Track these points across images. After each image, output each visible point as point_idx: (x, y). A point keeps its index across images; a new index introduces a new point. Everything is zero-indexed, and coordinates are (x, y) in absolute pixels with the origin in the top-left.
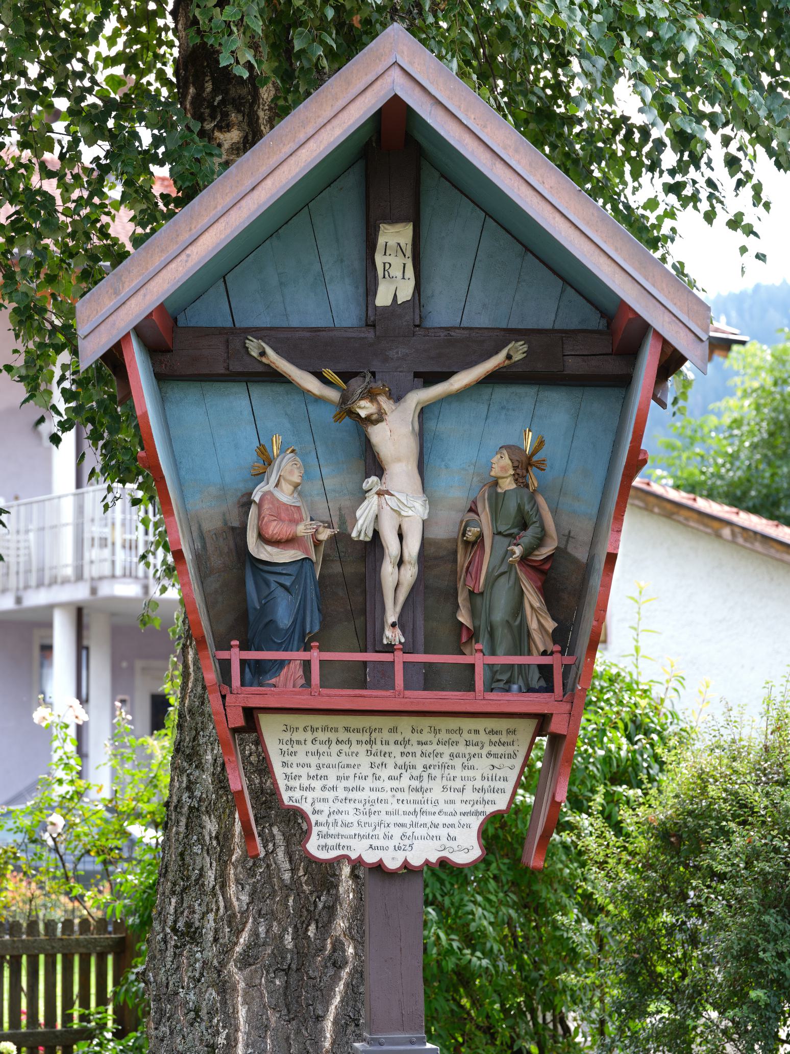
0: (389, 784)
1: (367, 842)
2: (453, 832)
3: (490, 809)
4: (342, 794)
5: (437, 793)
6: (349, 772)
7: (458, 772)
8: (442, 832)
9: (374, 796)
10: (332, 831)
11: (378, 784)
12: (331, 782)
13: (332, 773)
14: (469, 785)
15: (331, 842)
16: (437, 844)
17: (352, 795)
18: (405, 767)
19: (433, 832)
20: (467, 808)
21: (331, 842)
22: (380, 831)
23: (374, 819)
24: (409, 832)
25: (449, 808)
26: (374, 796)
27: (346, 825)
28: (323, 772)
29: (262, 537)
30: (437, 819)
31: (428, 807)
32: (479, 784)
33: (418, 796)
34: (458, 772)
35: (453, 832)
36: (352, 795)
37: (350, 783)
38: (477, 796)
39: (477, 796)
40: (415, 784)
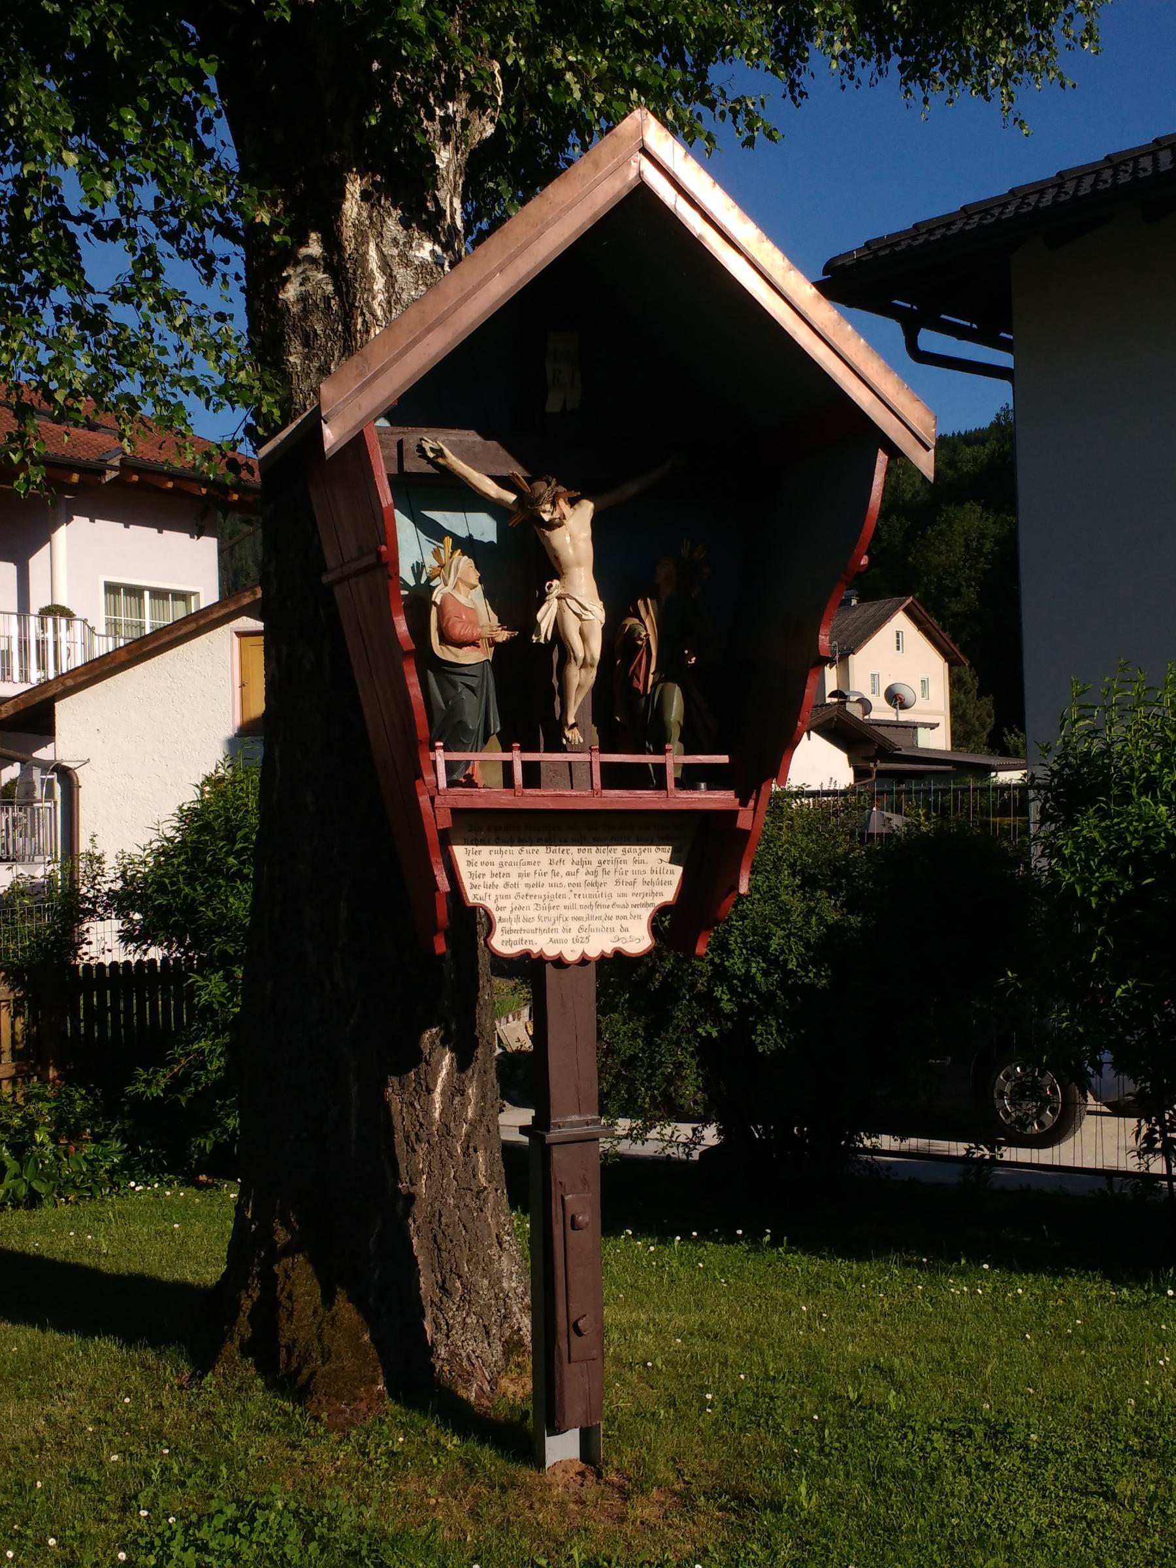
0: (567, 880)
1: (547, 936)
2: (625, 923)
3: (659, 901)
4: (523, 890)
5: (610, 888)
6: (530, 869)
7: (630, 867)
8: (615, 924)
9: (553, 891)
10: (515, 926)
11: (557, 880)
12: (513, 879)
13: (514, 871)
14: (640, 878)
15: (514, 937)
16: (610, 936)
17: (533, 891)
18: (582, 863)
19: (607, 924)
20: (638, 900)
21: (514, 937)
22: (559, 926)
23: (553, 913)
24: (586, 925)
25: (621, 901)
26: (553, 891)
27: (527, 920)
28: (506, 869)
29: (445, 639)
30: (614, 912)
31: (602, 901)
32: (648, 877)
33: (593, 890)
34: (630, 867)
35: (625, 923)
36: (533, 891)
37: (531, 880)
38: (646, 889)
39: (646, 889)
40: (591, 879)
